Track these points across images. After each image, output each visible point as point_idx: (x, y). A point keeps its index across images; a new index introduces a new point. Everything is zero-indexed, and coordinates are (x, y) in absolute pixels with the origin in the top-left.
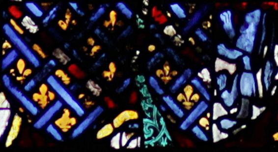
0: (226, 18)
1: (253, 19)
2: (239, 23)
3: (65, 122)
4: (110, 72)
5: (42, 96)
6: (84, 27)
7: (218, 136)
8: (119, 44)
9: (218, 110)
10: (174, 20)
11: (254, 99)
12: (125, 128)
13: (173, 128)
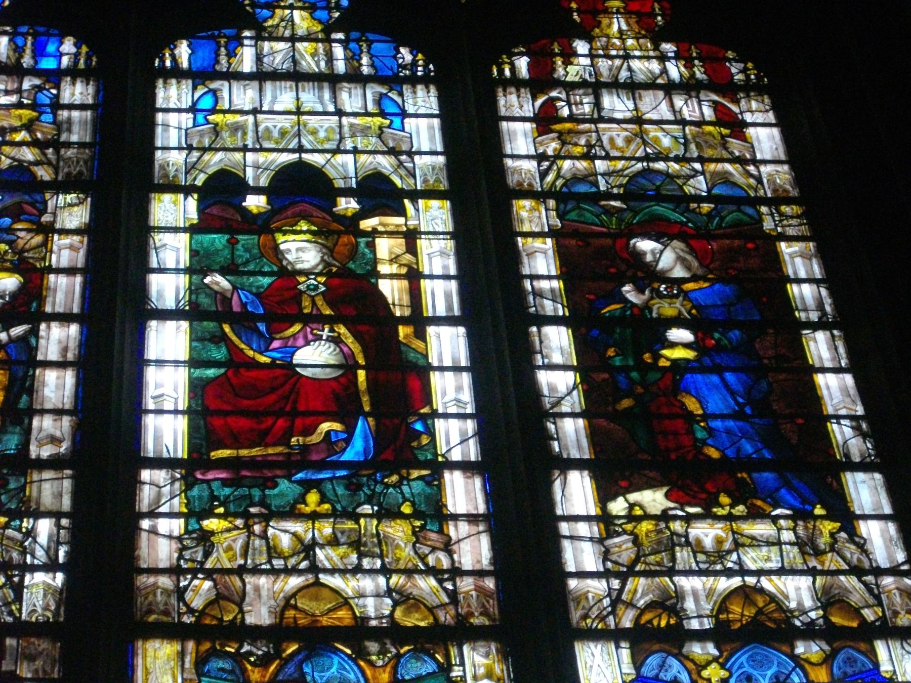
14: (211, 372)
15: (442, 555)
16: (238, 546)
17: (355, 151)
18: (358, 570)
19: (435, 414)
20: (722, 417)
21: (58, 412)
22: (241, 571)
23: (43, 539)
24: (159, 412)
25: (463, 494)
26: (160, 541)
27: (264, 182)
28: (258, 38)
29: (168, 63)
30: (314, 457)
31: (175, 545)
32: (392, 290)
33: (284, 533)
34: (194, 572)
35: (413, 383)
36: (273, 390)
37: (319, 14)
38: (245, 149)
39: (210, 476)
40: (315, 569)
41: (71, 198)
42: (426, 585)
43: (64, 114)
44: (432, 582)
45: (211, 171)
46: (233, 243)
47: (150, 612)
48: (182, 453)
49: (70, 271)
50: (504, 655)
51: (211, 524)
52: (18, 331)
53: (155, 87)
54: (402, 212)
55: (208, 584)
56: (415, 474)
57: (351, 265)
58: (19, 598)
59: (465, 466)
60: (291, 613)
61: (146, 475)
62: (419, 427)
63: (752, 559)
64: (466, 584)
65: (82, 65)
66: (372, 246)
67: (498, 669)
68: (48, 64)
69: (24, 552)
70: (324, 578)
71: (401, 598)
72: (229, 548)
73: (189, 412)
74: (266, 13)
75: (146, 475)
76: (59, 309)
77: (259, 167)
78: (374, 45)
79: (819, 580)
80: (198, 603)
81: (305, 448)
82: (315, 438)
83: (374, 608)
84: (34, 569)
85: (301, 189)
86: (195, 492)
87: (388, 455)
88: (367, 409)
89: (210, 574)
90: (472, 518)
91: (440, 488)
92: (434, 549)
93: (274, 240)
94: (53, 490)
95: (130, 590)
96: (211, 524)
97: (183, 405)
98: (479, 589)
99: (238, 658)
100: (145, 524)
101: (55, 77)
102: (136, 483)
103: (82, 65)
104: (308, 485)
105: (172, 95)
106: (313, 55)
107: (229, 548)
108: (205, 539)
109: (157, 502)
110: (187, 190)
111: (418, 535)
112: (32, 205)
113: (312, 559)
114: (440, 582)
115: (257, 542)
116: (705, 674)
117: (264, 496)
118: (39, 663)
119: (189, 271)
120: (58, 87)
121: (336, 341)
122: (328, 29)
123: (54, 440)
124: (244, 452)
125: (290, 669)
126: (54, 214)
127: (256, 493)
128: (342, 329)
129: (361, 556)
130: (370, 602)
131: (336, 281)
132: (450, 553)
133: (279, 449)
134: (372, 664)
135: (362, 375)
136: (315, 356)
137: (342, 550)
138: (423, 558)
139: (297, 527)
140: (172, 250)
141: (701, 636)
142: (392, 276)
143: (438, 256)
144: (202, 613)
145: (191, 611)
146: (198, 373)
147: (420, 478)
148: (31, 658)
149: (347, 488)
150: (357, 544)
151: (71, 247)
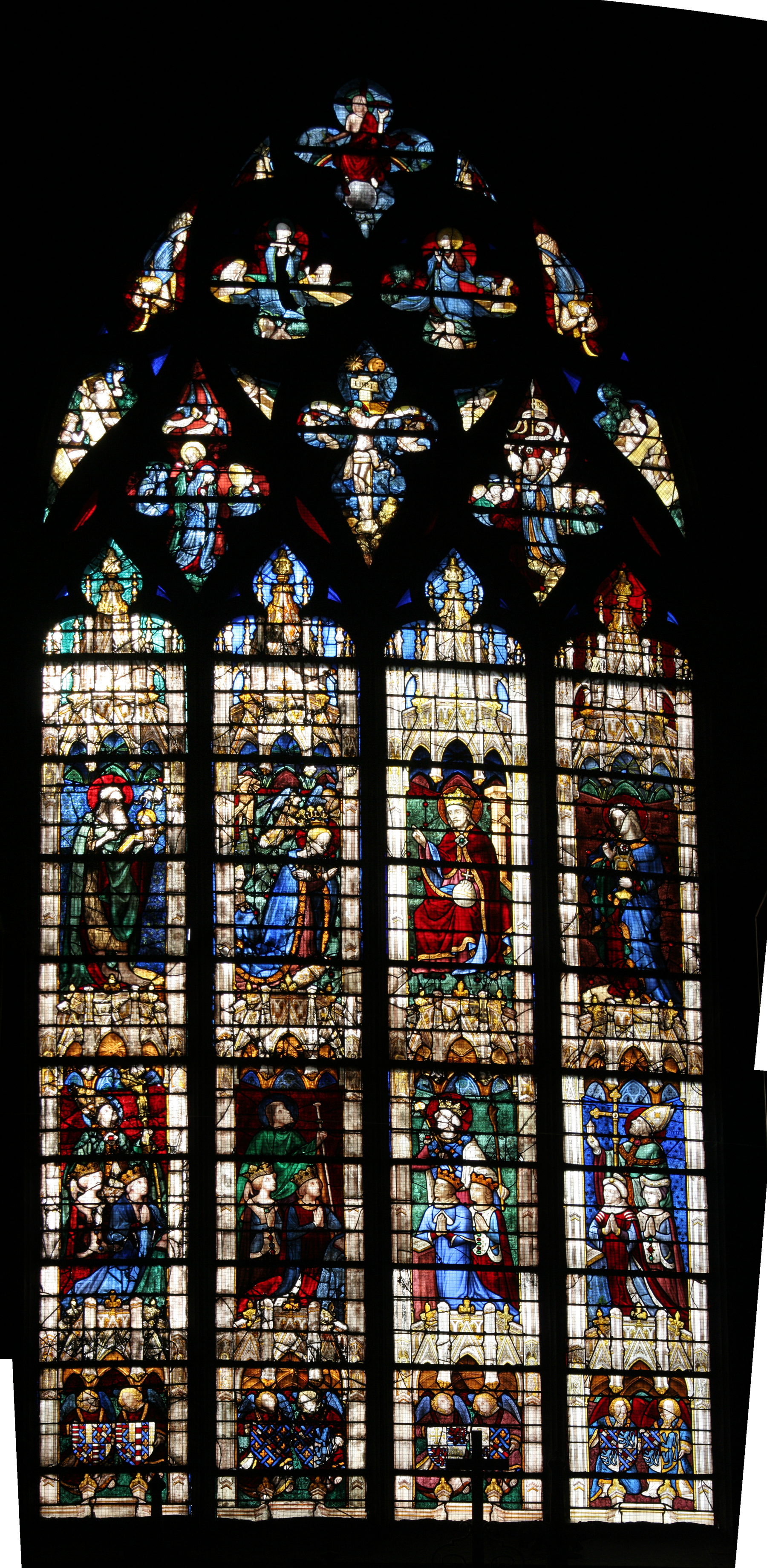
0: (318, 1430)
1: (326, 1430)
2: (322, 1432)
3: (270, 1461)
4: (283, 1447)
5: (263, 1454)
6: (275, 1432)
7: (316, 1466)
8: (286, 1438)
9: (316, 1458)
10: (302, 1431)
11: (326, 1455)
12: (288, 1463)
13: (302, 1463)
14: (417, 902)
15: (512, 1022)
16: (430, 1014)
17: (484, 732)
18: (478, 1031)
19: (513, 934)
20: (638, 940)
21: (352, 928)
22: (432, 1030)
23: (351, 1009)
24: (395, 929)
25: (524, 986)
26: (398, 1018)
27: (439, 759)
28: (437, 629)
29: (391, 652)
30: (462, 961)
31: (405, 1013)
32: (497, 842)
33: (449, 1006)
34: (413, 1029)
35: (506, 911)
36: (445, 914)
37: (469, 605)
38: (431, 730)
39: (419, 971)
40: (460, 1030)
41: (347, 770)
42: (506, 1039)
43: (341, 697)
44: (507, 1037)
45: (414, 747)
46: (425, 805)
47: (396, 1053)
48: (406, 958)
49: (352, 828)
50: (535, 1081)
51: (420, 1001)
52: (332, 872)
53: (385, 674)
54: (504, 784)
55: (418, 1037)
56: (504, 973)
57: (480, 824)
58: (343, 1045)
59: (524, 969)
60: (451, 1055)
61: (392, 970)
62: (506, 941)
63: (640, 1031)
64: (522, 1040)
65: (348, 655)
66: (489, 809)
67: (532, 1089)
68: (330, 652)
69: (343, 1017)
70: (465, 1035)
71: (496, 1047)
72: (426, 1016)
73: (409, 930)
74: (439, 604)
75: (392, 970)
76: (349, 857)
77: (437, 744)
78: (496, 636)
79: (664, 1045)
80: (414, 1048)
81: (458, 954)
82: (462, 948)
83: (484, 1052)
84: (348, 1028)
85: (457, 754)
86: (412, 981)
87: (492, 960)
88: (485, 929)
89: (419, 1031)
90: (526, 1002)
91: (514, 981)
92: (510, 1019)
93: (444, 804)
94: (354, 978)
95: (386, 1040)
96: (420, 1001)
97: (406, 927)
98: (527, 1043)
99: (431, 1079)
100: (392, 1000)
101: (334, 664)
102: (387, 975)
103: (348, 655)
104: (460, 978)
105: (395, 680)
106: (465, 644)
107: (426, 1016)
108: (416, 1009)
109: (396, 988)
110: (402, 764)
111: (504, 1009)
112: (331, 775)
113: (459, 1022)
114: (511, 1038)
115: (438, 1012)
116: (611, 1095)
117: (440, 984)
118: (353, 1081)
119: (406, 829)
120: (337, 673)
121: (472, 880)
122: (474, 620)
123: (352, 947)
124: (432, 956)
125: (451, 1086)
126: (342, 782)
127: (437, 981)
128: (475, 873)
129: (480, 1022)
130: (482, 1049)
131: (473, 836)
132: (516, 1021)
133: (447, 955)
134: (482, 1084)
135: (483, 903)
136: (462, 892)
137: (472, 1018)
138: (505, 1024)
139: (454, 1003)
140: (397, 812)
141: (612, 1075)
142: (498, 834)
143: (520, 821)
144: (416, 1054)
145: (412, 1052)
146: (412, 902)
147: (506, 975)
148: (350, 1079)
149: (475, 980)
150: (478, 1016)
151: (352, 810)
